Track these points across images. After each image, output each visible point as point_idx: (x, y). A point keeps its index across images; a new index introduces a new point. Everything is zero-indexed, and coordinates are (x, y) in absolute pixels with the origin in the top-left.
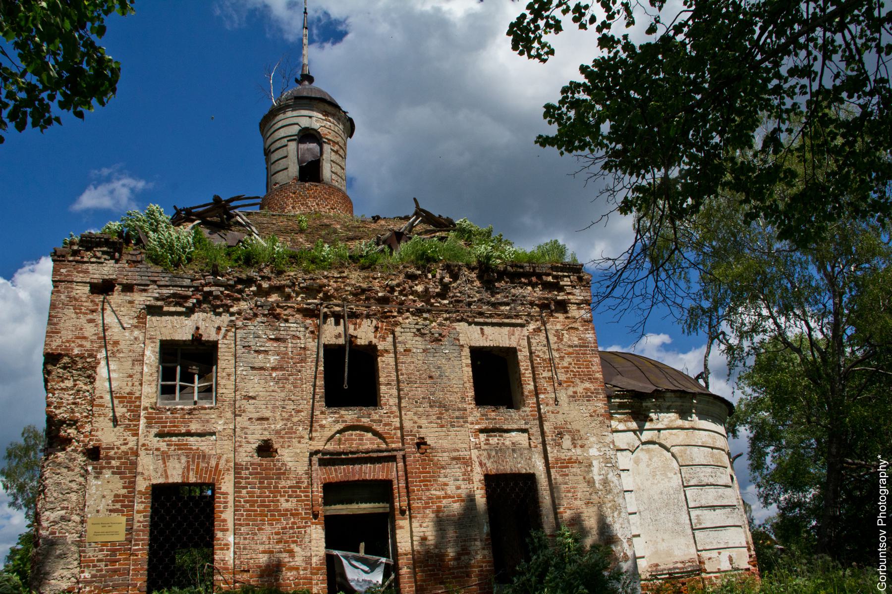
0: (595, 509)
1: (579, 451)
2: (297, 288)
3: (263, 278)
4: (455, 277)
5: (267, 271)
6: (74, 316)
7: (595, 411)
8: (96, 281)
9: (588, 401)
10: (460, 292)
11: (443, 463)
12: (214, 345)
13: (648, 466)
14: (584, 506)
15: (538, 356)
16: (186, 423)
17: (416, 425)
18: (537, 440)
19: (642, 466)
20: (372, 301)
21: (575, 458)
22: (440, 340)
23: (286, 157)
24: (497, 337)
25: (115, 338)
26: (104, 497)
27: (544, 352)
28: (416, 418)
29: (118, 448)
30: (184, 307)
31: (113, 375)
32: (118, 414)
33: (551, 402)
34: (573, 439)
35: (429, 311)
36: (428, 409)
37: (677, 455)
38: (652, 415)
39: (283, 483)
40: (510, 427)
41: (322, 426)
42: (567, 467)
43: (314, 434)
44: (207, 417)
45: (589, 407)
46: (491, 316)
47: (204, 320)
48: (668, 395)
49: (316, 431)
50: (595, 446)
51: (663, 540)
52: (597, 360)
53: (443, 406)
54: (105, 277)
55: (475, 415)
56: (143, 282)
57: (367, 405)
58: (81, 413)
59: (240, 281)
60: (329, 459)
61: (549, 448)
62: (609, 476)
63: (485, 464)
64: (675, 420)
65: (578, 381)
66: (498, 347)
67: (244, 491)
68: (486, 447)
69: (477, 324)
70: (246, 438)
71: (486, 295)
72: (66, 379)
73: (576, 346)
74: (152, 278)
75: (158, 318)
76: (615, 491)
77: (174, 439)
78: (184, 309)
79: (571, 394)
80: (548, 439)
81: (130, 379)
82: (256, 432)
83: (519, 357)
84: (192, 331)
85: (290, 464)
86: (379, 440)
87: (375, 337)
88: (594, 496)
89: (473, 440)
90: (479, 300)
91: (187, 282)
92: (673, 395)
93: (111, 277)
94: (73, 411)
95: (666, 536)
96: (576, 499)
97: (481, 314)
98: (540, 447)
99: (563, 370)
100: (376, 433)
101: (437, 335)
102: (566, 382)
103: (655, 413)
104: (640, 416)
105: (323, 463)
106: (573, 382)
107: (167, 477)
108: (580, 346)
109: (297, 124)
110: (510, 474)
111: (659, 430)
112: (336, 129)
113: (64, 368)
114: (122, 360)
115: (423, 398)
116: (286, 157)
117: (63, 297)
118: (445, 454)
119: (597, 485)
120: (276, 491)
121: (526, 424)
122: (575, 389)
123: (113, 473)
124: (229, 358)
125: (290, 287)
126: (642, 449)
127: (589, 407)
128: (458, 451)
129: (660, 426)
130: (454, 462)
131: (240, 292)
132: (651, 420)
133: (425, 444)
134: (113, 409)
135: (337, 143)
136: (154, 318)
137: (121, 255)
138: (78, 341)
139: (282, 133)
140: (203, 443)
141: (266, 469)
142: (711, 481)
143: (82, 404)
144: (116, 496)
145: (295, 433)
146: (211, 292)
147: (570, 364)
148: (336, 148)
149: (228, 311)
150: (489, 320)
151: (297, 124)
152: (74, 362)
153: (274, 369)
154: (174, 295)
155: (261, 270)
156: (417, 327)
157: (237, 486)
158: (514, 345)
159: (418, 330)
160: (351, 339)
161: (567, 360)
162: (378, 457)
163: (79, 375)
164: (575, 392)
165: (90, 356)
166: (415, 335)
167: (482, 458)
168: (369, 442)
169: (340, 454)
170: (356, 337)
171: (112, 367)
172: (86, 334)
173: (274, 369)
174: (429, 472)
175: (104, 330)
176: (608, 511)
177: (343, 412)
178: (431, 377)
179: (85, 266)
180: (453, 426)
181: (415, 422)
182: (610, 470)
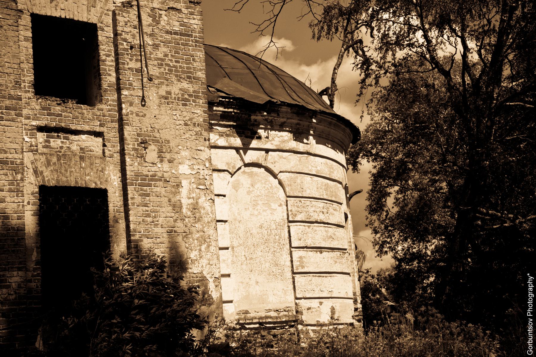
1: (166, 166)
7: (191, 119)
9: (185, 105)
13: (249, 193)
15: (125, 40)
18: (113, 148)
19: (242, 192)
21: (159, 174)
27: (134, 36)
33: (137, 101)
34: (160, 151)
37: (285, 183)
38: (261, 132)
40: (79, 128)
42: (149, 185)
45: (185, 114)
48: (284, 109)
50: (187, 162)
51: (257, 283)
52: (200, 55)
55: (35, 109)
61: (128, 160)
62: (200, 201)
63: (42, 172)
64: (288, 141)
65: (174, 79)
73: (176, 33)
76: (206, 220)
79: (164, 94)
80: (129, 147)
83: (100, 38)
88: (179, 224)
96: (156, 225)
98: (117, 156)
99: (156, 63)
102: (158, 78)
103: (265, 129)
104: (247, 131)
108: (182, 34)
110: (75, 188)
111: (267, 151)
119: (184, 210)
121: (101, 125)
122: (168, 89)
126: (244, 172)
129: (268, 146)
132: (259, 138)
147: (166, 55)
161: (163, 49)
164: (169, 93)
167: (39, 164)
182: (202, 193)
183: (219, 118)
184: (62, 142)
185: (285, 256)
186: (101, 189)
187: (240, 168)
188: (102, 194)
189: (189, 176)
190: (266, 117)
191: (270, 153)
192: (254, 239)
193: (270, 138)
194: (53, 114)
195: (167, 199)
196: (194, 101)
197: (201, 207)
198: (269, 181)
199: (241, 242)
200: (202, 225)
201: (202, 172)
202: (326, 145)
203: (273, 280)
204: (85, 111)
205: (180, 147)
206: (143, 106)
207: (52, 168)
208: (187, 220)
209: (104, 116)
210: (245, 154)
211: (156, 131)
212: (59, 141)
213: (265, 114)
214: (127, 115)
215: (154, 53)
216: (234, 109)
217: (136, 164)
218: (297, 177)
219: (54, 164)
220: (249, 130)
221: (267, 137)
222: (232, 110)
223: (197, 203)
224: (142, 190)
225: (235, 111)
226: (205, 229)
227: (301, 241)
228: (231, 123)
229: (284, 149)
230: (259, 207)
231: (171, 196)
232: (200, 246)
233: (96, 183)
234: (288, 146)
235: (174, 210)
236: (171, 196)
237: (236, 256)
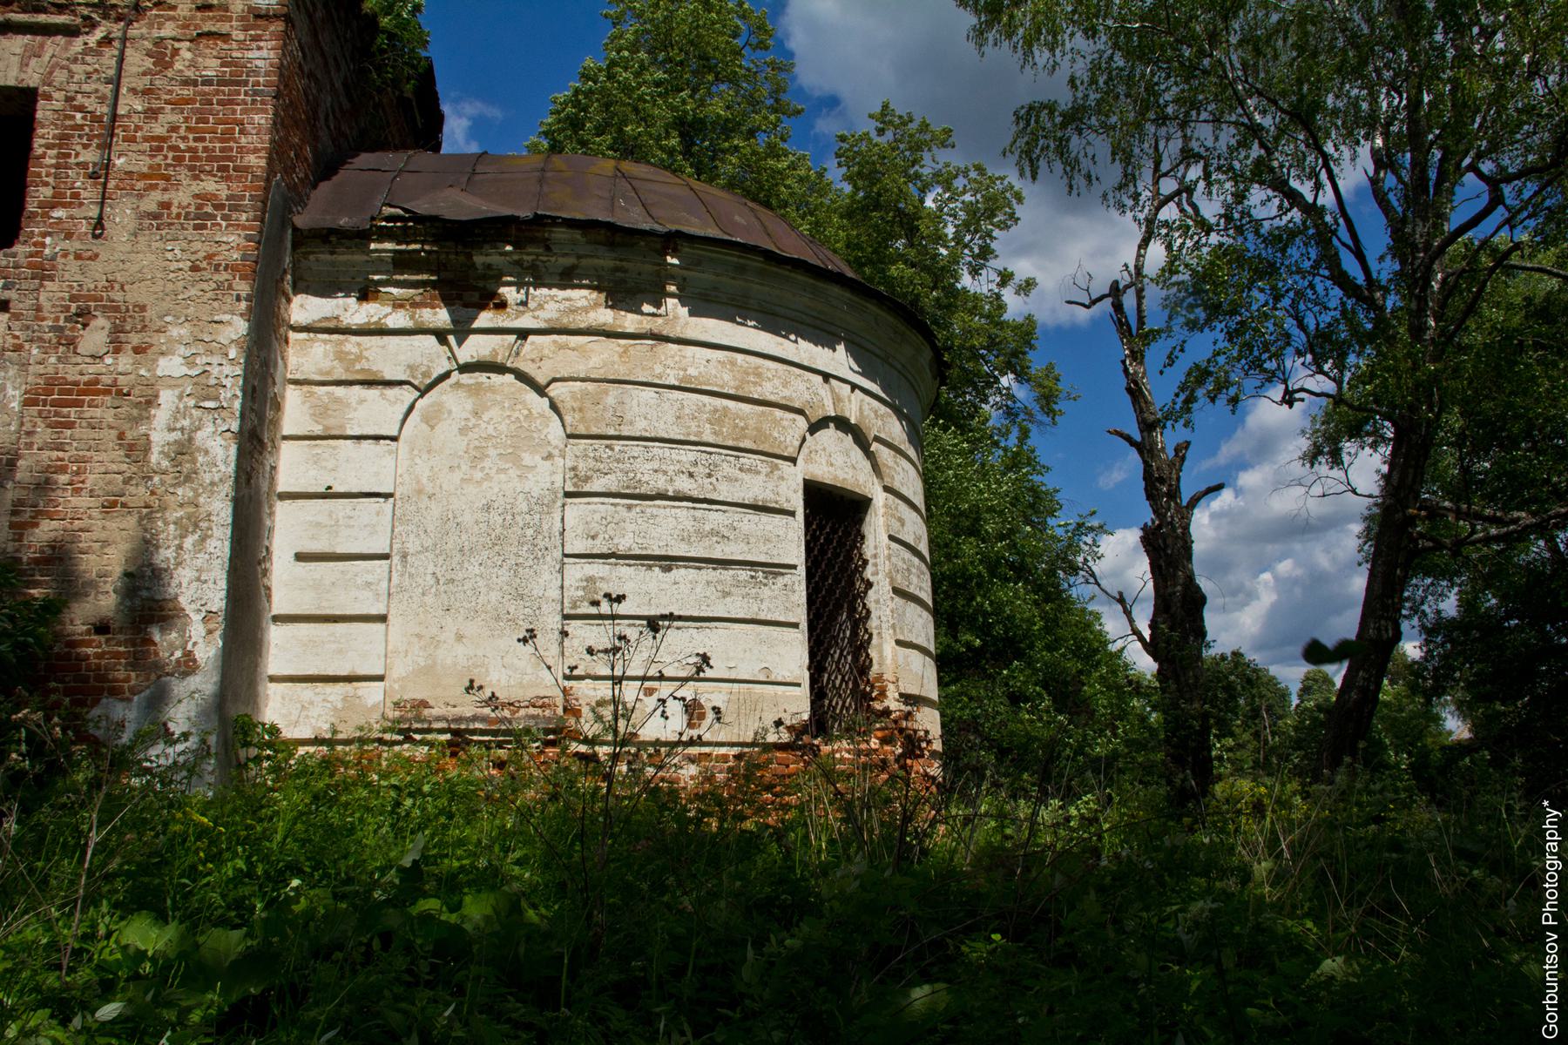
0: (131, 522)
1: (125, 362)
7: (209, 257)
9: (196, 227)
13: (463, 431)
14: (95, 513)
19: (446, 431)
37: (566, 404)
38: (509, 293)
45: (197, 246)
48: (560, 234)
50: (182, 350)
64: (586, 310)
65: (183, 174)
76: (207, 478)
79: (153, 207)
92: (577, 235)
95: (471, 629)
103: (519, 285)
104: (467, 293)
106: (167, 178)
111: (523, 334)
119: (154, 457)
122: (166, 197)
126: (458, 385)
127: (197, 246)
132: (502, 305)
142: (684, 485)
161: (169, 117)
164: (166, 205)
176: (168, 532)
182: (208, 418)
183: (391, 267)
185: (546, 576)
187: (447, 375)
189: (180, 382)
190: (516, 257)
191: (531, 338)
192: (464, 537)
193: (532, 305)
195: (114, 433)
196: (225, 218)
197: (199, 449)
198: (523, 403)
199: (429, 543)
200: (193, 489)
201: (215, 371)
202: (733, 321)
203: (507, 632)
205: (168, 319)
206: (95, 237)
208: (156, 479)
210: (460, 343)
211: (117, 286)
213: (509, 248)
215: (146, 127)
216: (423, 243)
218: (606, 392)
220: (475, 289)
221: (524, 303)
222: (418, 246)
223: (190, 440)
225: (427, 247)
226: (201, 500)
227: (598, 542)
228: (425, 277)
229: (572, 326)
230: (487, 463)
231: (126, 426)
232: (182, 537)
234: (582, 321)
235: (127, 456)
236: (126, 426)
237: (411, 575)
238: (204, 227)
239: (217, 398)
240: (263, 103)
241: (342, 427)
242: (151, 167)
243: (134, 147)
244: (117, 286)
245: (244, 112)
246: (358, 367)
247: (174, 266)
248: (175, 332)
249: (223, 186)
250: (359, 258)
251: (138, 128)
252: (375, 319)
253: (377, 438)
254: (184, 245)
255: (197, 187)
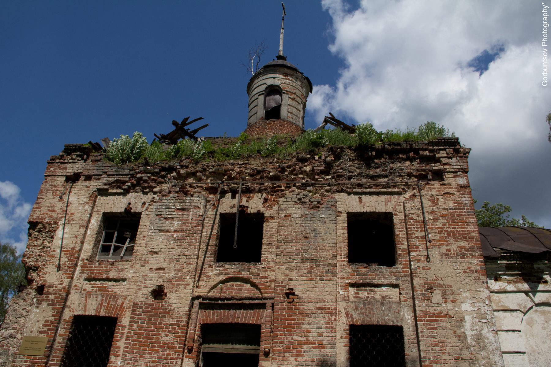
1: (450, 306)
2: (207, 173)
3: (182, 167)
4: (338, 157)
5: (185, 162)
6: (51, 197)
7: (469, 268)
8: (69, 174)
9: (461, 258)
10: (342, 169)
11: (308, 312)
12: (138, 216)
15: (412, 219)
16: (107, 271)
17: (287, 278)
18: (407, 295)
20: (266, 179)
21: (444, 312)
22: (319, 207)
23: (257, 106)
24: (373, 204)
25: (72, 211)
26: (38, 321)
27: (418, 215)
28: (288, 272)
29: (56, 287)
30: (122, 189)
31: (66, 236)
32: (61, 263)
33: (423, 259)
35: (312, 185)
36: (299, 264)
39: (166, 321)
40: (380, 282)
41: (208, 277)
42: (437, 321)
43: (201, 283)
44: (123, 267)
45: (463, 264)
46: (370, 187)
47: (135, 198)
49: (203, 280)
50: (469, 301)
52: (473, 221)
53: (315, 262)
54: (76, 172)
55: (346, 271)
56: (98, 174)
57: (249, 260)
58: (42, 262)
59: (163, 169)
60: (209, 304)
61: (417, 302)
62: (483, 332)
63: (351, 315)
65: (452, 240)
66: (375, 212)
67: (135, 325)
68: (355, 300)
69: (356, 194)
70: (145, 283)
71: (364, 170)
72: (39, 239)
73: (451, 209)
74: (104, 171)
75: (105, 198)
77: (97, 282)
78: (122, 191)
79: (445, 251)
80: (418, 293)
81: (75, 238)
82: (153, 279)
83: (395, 221)
84: (125, 206)
85: (174, 305)
86: (256, 291)
87: (264, 207)
89: (341, 292)
90: (359, 174)
91: (127, 171)
93: (79, 171)
94: (37, 261)
97: (360, 185)
98: (410, 301)
99: (437, 230)
100: (253, 285)
101: (315, 203)
102: (439, 241)
105: (202, 306)
107: (85, 310)
109: (265, 84)
110: (376, 325)
112: (294, 85)
113: (39, 231)
114: (73, 225)
115: (297, 255)
116: (257, 106)
117: (48, 186)
118: (310, 304)
120: (159, 327)
121: (397, 279)
122: (448, 248)
123: (49, 305)
124: (147, 224)
125: (201, 172)
127: (463, 264)
128: (324, 301)
130: (319, 312)
131: (163, 177)
133: (294, 294)
134: (60, 259)
135: (295, 94)
136: (102, 198)
137: (88, 158)
138: (50, 214)
139: (256, 91)
140: (117, 287)
141: (156, 308)
143: (43, 256)
144: (47, 321)
145: (183, 281)
146: (141, 177)
147: (444, 225)
148: (293, 96)
149: (152, 191)
150: (367, 190)
151: (265, 84)
152: (45, 227)
153: (176, 231)
154: (117, 181)
155: (181, 161)
156: (298, 197)
157: (132, 322)
158: (390, 209)
159: (299, 199)
160: (242, 209)
161: (442, 221)
162: (250, 304)
163: (47, 236)
164: (449, 250)
165: (55, 223)
166: (296, 203)
167: (349, 310)
168: (246, 291)
169: (219, 299)
170: (247, 207)
171: (66, 230)
172: (56, 209)
173: (176, 231)
174: (294, 320)
175: (67, 206)
177: (227, 266)
178: (306, 238)
179: (65, 165)
180: (322, 279)
181: (287, 275)
182: (484, 326)
183: (505, 269)
184: (368, 294)
186: (397, 326)
188: (399, 330)
189: (471, 312)
194: (361, 274)
195: (452, 332)
196: (470, 254)
201: (483, 308)
204: (384, 271)
205: (461, 290)
206: (429, 262)
207: (359, 312)
209: (399, 272)
211: (440, 279)
212: (366, 293)
214: (415, 270)
215: (435, 224)
216: (516, 260)
217: (424, 305)
219: (361, 309)
222: (515, 262)
223: (481, 334)
224: (430, 325)
225: (518, 262)
228: (517, 272)
233: (393, 322)
236: (456, 329)
238: (464, 258)
239: (486, 318)
240: (471, 215)
241: (500, 327)
242: (440, 238)
243: (433, 231)
244: (440, 279)
245: (466, 218)
246: (500, 305)
247: (458, 271)
248: (464, 295)
249: (466, 243)
250: (494, 266)
251: (432, 225)
252: (502, 288)
253: (514, 331)
254: (459, 264)
255: (458, 244)
